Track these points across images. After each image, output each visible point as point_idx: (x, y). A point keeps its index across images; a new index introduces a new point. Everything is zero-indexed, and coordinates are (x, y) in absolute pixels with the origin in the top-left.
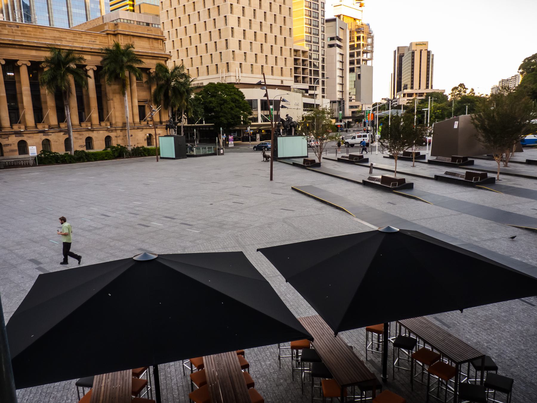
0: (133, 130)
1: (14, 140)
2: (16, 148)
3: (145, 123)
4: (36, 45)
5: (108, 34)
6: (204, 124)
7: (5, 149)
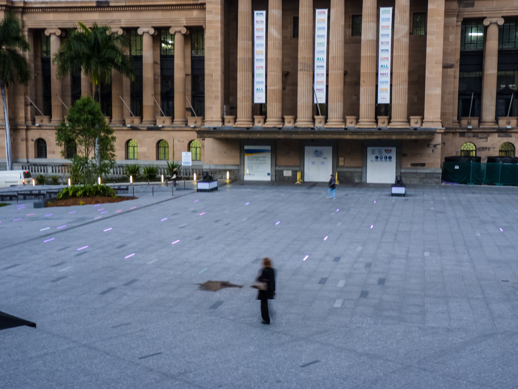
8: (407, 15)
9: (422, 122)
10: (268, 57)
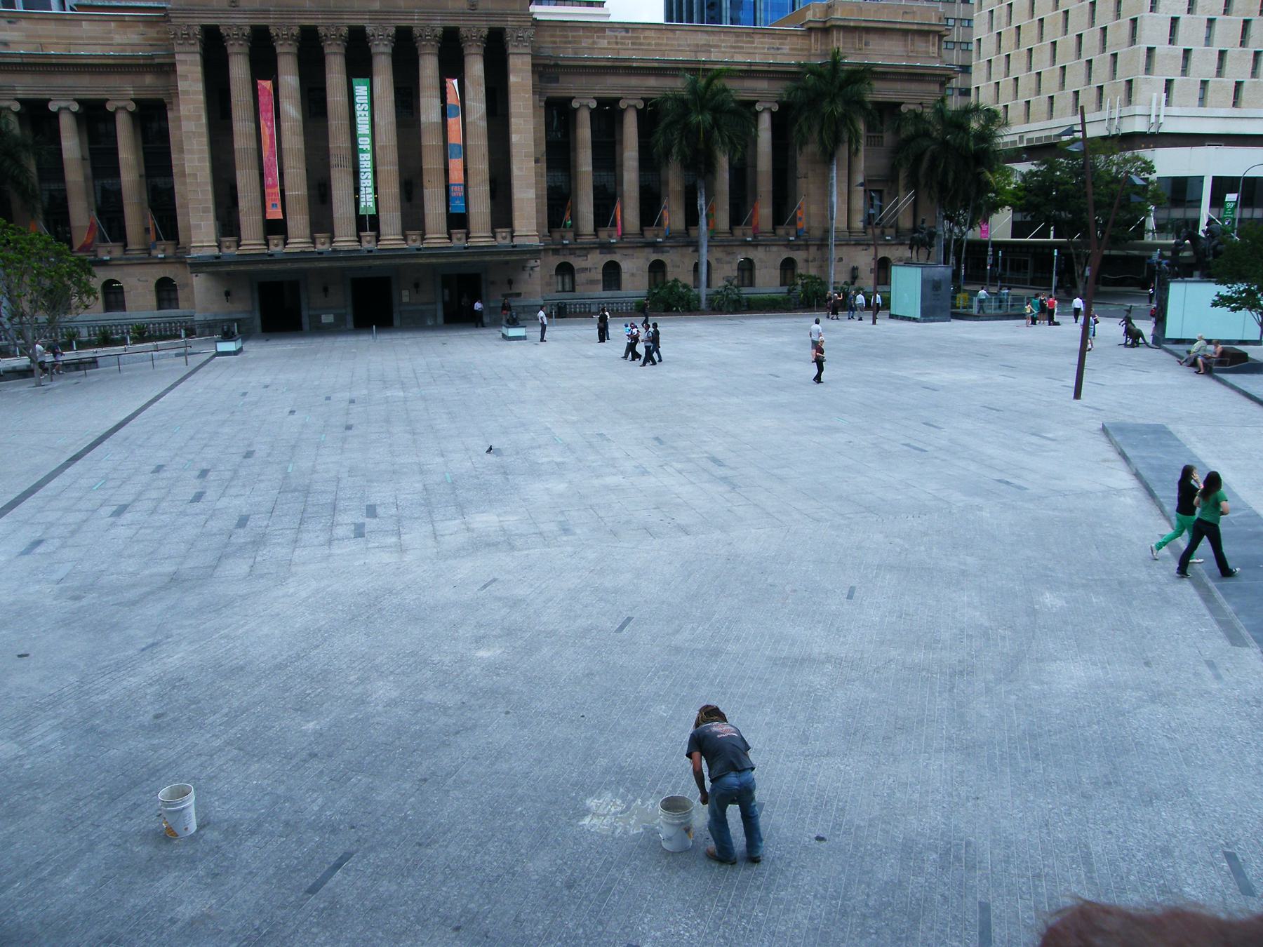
0: (845, 249)
1: (595, 262)
2: (600, 277)
3: (878, 231)
4: (656, 65)
5: (810, 29)
6: (1052, 239)
7: (579, 278)
8: (482, 89)
9: (512, 237)
10: (285, 145)
